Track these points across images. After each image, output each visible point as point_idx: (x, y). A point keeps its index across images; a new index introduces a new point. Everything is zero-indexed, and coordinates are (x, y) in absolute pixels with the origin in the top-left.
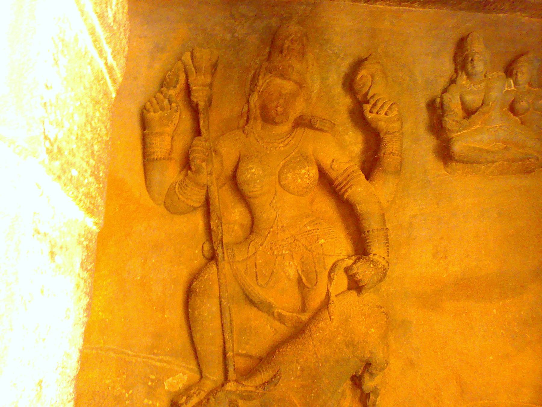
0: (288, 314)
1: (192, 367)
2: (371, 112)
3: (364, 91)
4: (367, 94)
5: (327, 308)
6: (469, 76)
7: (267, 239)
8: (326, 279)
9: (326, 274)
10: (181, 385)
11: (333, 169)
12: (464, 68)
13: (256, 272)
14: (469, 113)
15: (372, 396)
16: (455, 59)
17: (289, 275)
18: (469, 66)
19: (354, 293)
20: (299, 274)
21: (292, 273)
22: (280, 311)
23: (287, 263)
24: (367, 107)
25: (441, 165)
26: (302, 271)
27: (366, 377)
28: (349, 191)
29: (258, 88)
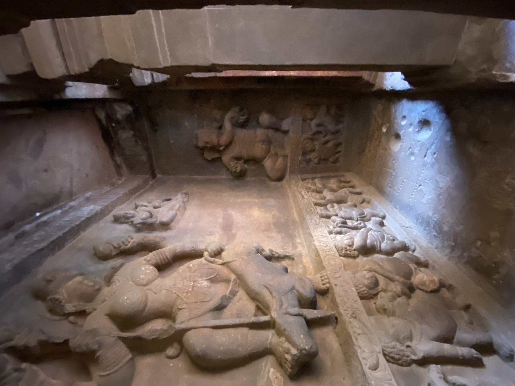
0: (230, 287)
1: (264, 364)
2: (127, 245)
3: (112, 248)
4: (115, 247)
5: (229, 263)
6: (133, 217)
7: (180, 295)
8: (213, 265)
9: (210, 264)
10: (278, 375)
11: (150, 260)
12: (128, 218)
13: (200, 302)
14: (151, 216)
15: (274, 253)
16: (122, 223)
17: (208, 286)
18: (129, 215)
19: (223, 254)
20: (207, 280)
21: (205, 284)
22: (228, 292)
23: (199, 285)
24: (123, 247)
25: (169, 231)
26: (206, 277)
27: (264, 253)
28: (166, 254)
29: (63, 301)
